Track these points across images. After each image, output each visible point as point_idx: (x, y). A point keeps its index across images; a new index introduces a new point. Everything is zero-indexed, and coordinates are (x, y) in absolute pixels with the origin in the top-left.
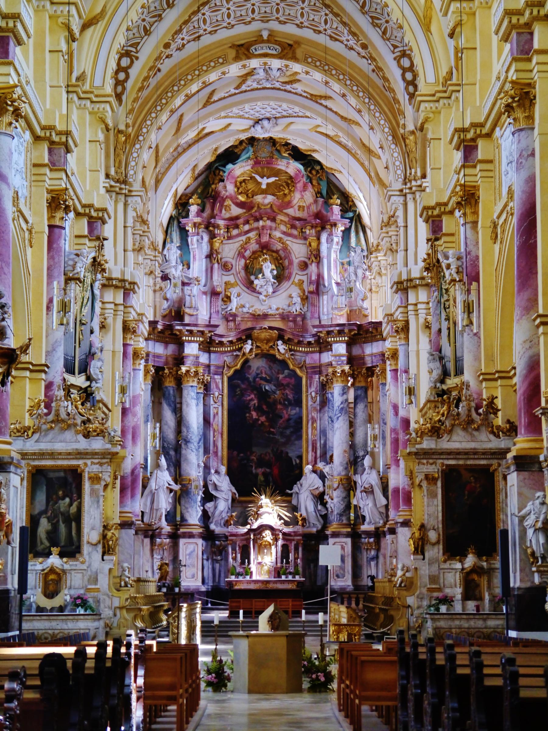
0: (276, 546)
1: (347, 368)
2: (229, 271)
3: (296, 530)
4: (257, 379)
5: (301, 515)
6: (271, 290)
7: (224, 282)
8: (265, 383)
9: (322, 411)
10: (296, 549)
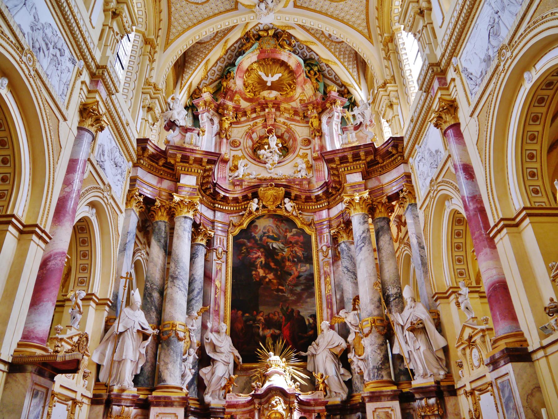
1: (366, 195)
2: (237, 147)
3: (316, 397)
4: (264, 238)
5: (322, 376)
6: (276, 158)
7: (232, 155)
8: (273, 241)
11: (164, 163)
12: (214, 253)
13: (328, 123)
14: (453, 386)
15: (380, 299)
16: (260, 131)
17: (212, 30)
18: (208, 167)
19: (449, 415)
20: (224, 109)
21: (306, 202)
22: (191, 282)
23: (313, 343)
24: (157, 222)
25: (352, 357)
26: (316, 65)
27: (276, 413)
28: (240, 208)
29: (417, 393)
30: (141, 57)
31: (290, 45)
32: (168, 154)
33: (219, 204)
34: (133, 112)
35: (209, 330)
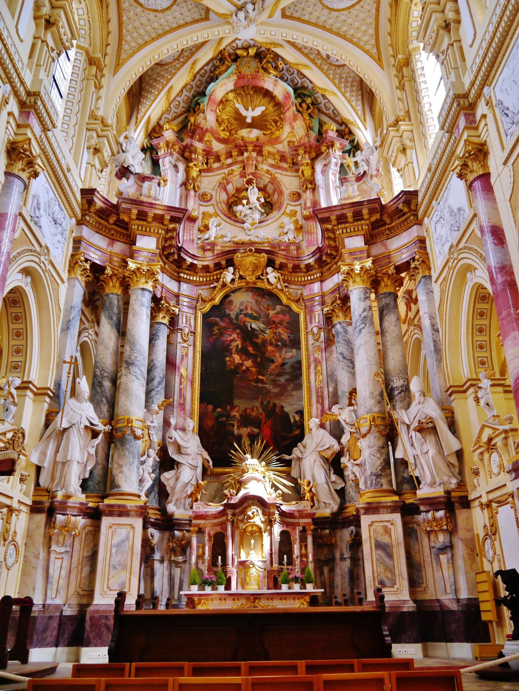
0: (271, 534)
1: (368, 263)
2: (208, 201)
3: (301, 508)
4: (241, 316)
5: (309, 483)
6: (257, 216)
7: (201, 212)
8: (251, 320)
9: (328, 350)
10: (303, 540)
11: (116, 221)
12: (179, 334)
13: (323, 172)
14: (467, 497)
15: (382, 392)
16: (237, 181)
17: (175, 47)
18: (171, 226)
19: (459, 531)
20: (191, 152)
21: (293, 272)
22: (150, 369)
23: (299, 444)
24: (107, 295)
25: (346, 462)
26: (310, 96)
27: (252, 526)
28: (212, 278)
29: (423, 504)
30: (85, 82)
31: (276, 68)
32: (121, 209)
33: (184, 274)
34: (75, 154)
35: (172, 427)
